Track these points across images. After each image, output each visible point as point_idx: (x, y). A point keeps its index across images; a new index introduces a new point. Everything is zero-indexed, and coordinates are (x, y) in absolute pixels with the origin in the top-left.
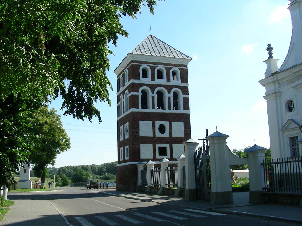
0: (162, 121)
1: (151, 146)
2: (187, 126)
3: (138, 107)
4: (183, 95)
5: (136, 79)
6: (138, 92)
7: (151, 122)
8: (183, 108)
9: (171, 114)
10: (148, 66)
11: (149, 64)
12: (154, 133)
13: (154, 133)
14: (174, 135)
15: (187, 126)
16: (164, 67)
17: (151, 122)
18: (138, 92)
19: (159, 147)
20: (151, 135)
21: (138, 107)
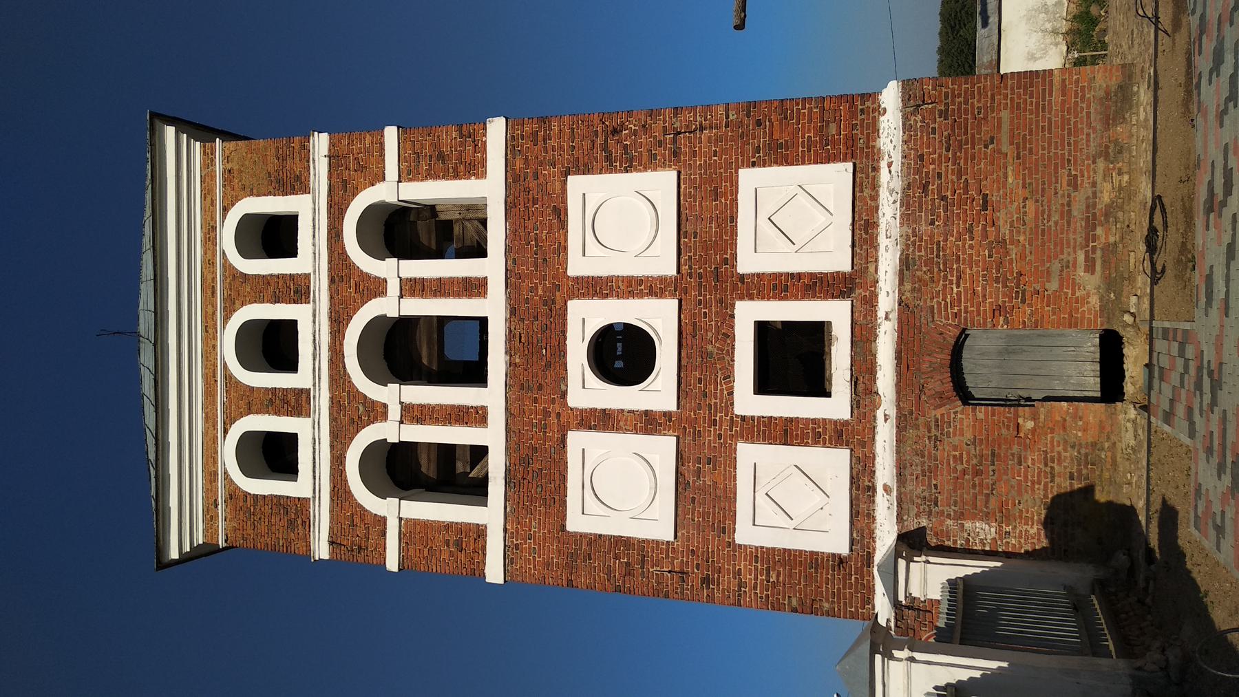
0: (561, 352)
1: (748, 454)
2: (599, 141)
3: (479, 532)
4: (384, 179)
5: (307, 524)
6: (384, 519)
7: (577, 440)
8: (473, 182)
9: (512, 279)
10: (226, 432)
11: (215, 426)
12: (649, 423)
13: (649, 423)
14: (664, 263)
15: (599, 141)
16: (226, 318)
17: (577, 440)
18: (384, 519)
19: (764, 385)
20: (663, 448)
21: (479, 532)
